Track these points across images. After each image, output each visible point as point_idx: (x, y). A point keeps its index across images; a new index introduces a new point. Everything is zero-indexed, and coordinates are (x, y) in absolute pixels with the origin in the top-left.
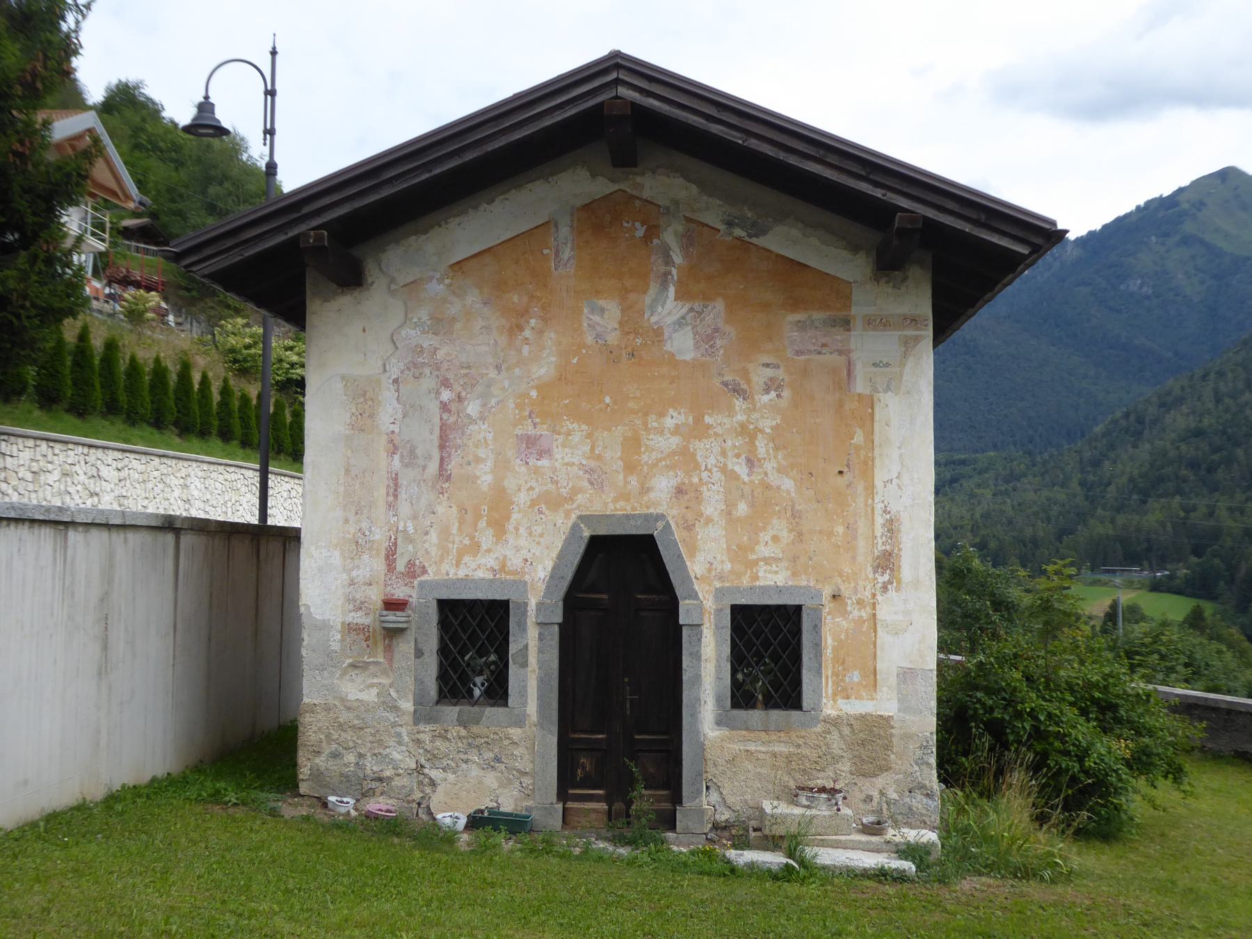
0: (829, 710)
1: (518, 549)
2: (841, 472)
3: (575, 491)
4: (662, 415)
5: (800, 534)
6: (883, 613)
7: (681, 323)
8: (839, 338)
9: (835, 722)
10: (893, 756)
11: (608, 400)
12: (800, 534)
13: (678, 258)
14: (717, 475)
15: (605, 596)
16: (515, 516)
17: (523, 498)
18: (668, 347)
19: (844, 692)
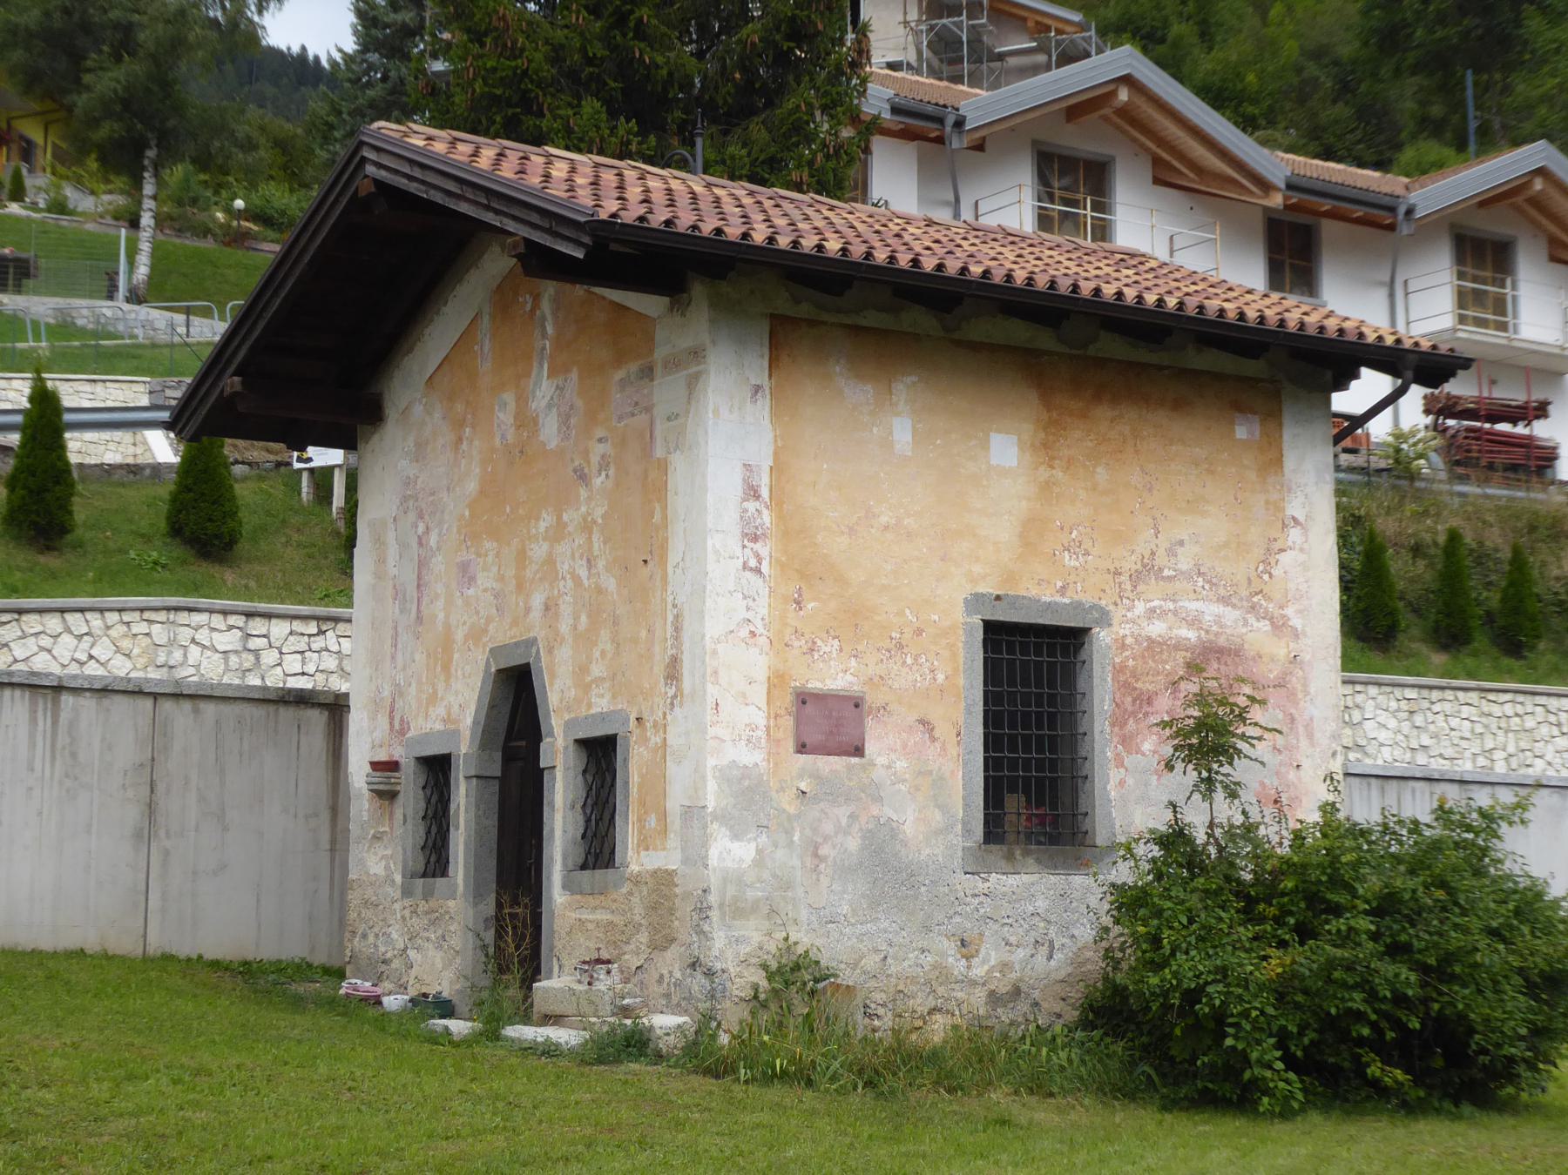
0: (634, 868)
1: (457, 693)
2: (645, 561)
3: (489, 620)
4: (538, 519)
5: (618, 644)
6: (674, 739)
7: (549, 406)
8: (646, 391)
9: (637, 880)
10: (676, 923)
11: (508, 510)
12: (618, 644)
13: (550, 330)
14: (570, 583)
15: (524, 743)
16: (456, 656)
17: (459, 635)
18: (541, 438)
19: (645, 844)
